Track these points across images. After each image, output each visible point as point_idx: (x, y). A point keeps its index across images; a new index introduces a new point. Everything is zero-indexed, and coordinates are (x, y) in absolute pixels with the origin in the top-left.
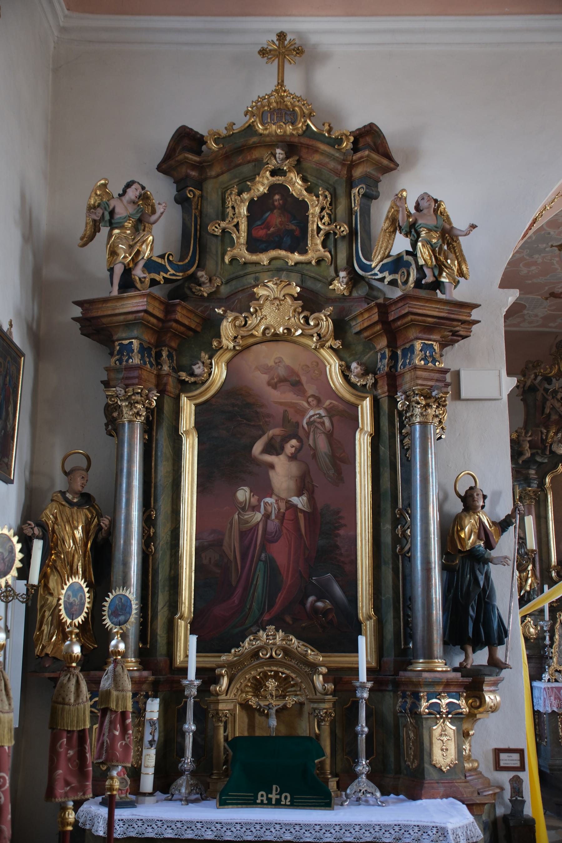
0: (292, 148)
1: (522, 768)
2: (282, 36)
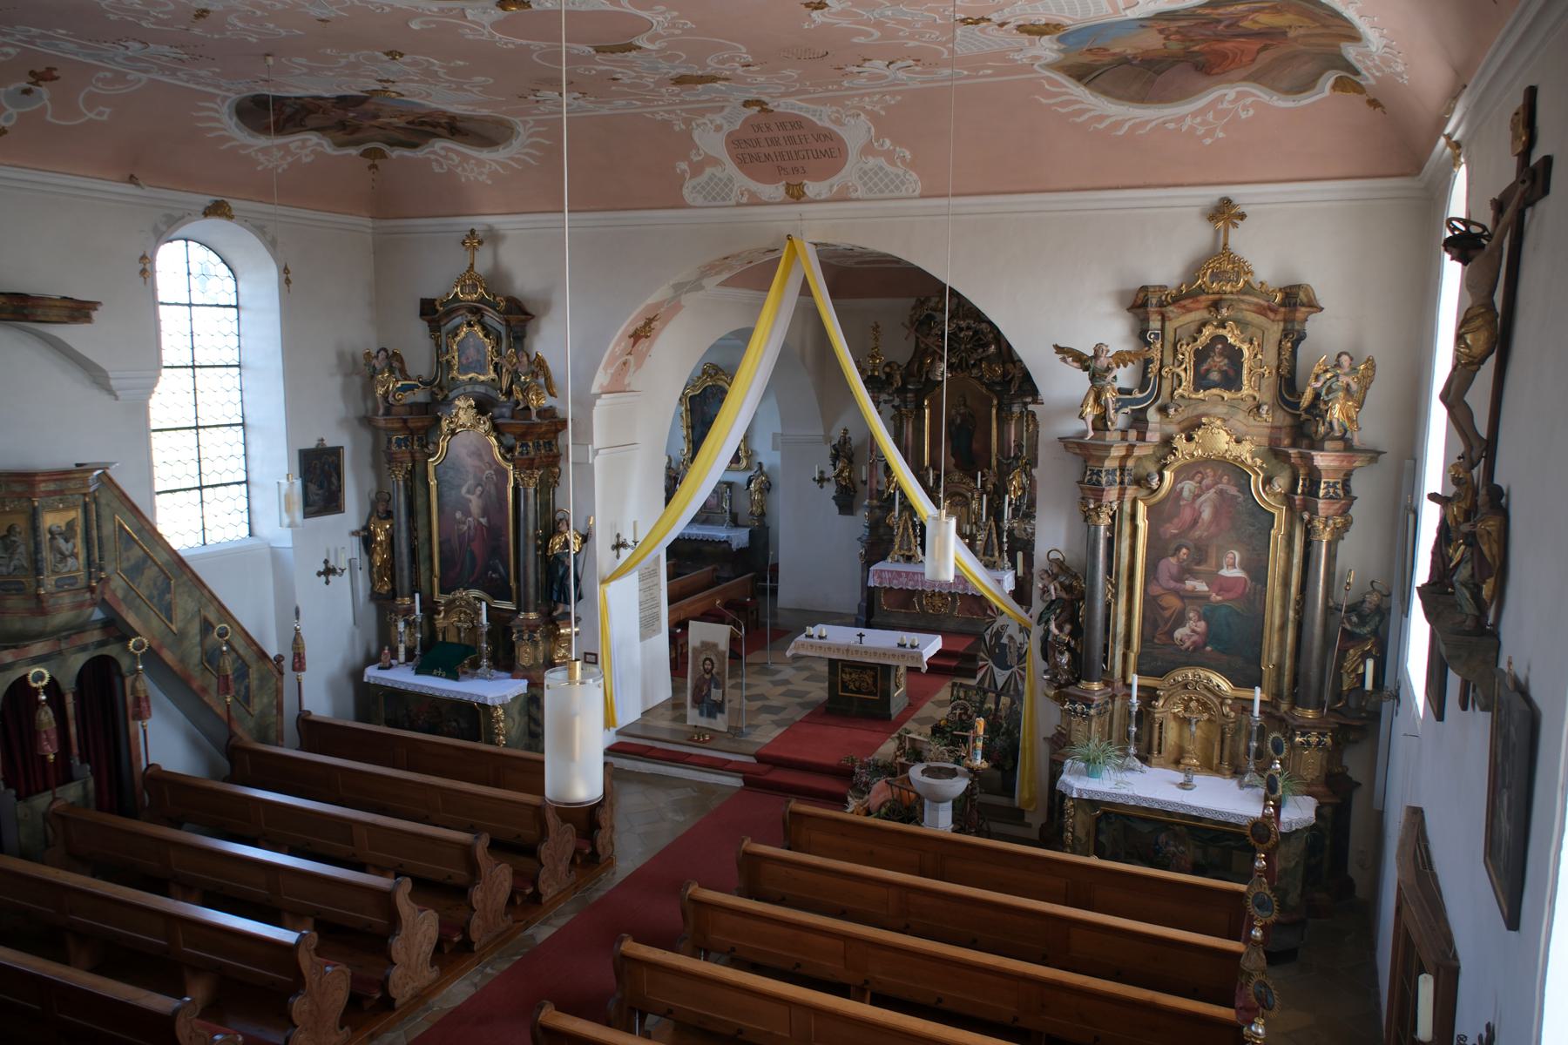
0: (476, 311)
2: (472, 232)
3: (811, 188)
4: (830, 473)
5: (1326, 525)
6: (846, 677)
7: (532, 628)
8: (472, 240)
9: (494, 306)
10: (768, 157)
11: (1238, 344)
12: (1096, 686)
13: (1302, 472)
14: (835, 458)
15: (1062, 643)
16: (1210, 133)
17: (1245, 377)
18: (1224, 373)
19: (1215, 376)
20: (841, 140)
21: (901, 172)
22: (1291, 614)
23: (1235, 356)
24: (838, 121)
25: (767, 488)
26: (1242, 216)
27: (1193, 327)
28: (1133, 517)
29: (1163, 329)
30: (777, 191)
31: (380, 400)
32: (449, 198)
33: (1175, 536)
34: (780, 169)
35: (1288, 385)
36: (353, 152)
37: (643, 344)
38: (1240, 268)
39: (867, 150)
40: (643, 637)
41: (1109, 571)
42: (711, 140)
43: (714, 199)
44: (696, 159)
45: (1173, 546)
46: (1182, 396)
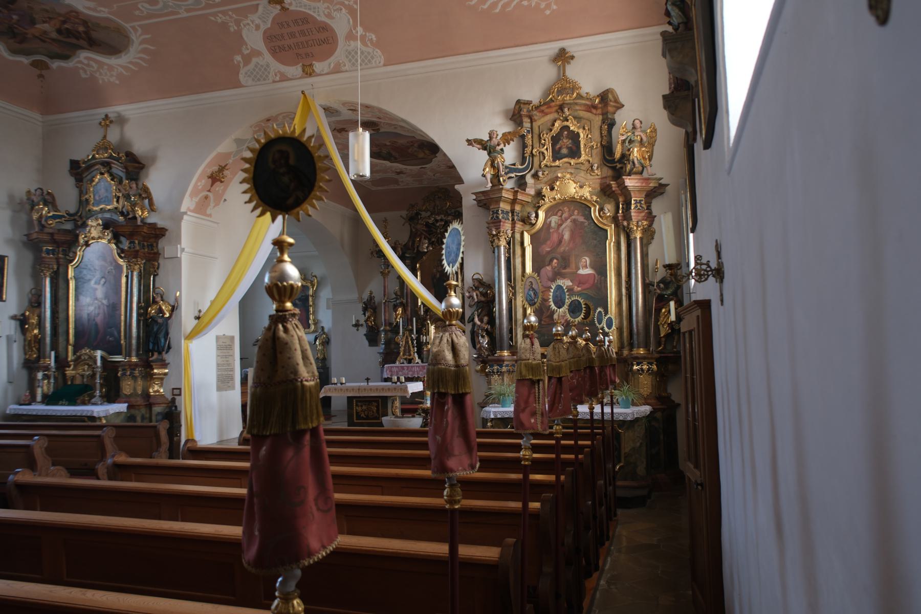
0: (107, 164)
1: (180, 395)
2: (107, 116)
3: (318, 66)
4: (362, 320)
5: (637, 226)
6: (359, 409)
7: (133, 366)
8: (107, 122)
9: (118, 159)
10: (290, 47)
11: (576, 130)
12: (506, 353)
13: (621, 199)
14: (365, 310)
15: (483, 330)
16: (548, 6)
17: (582, 149)
18: (570, 149)
19: (564, 151)
20: (332, 30)
21: (371, 50)
22: (624, 291)
23: (575, 137)
24: (329, 16)
25: (326, 342)
26: (572, 57)
27: (549, 124)
28: (522, 243)
29: (532, 128)
30: (296, 70)
31: (36, 223)
32: (93, 95)
33: (548, 252)
34: (298, 55)
35: (607, 149)
36: (25, 60)
37: (218, 187)
38: (574, 87)
39: (350, 37)
40: (219, 389)
41: (509, 279)
42: (254, 39)
43: (259, 80)
44: (246, 52)
45: (548, 259)
46: (546, 166)
